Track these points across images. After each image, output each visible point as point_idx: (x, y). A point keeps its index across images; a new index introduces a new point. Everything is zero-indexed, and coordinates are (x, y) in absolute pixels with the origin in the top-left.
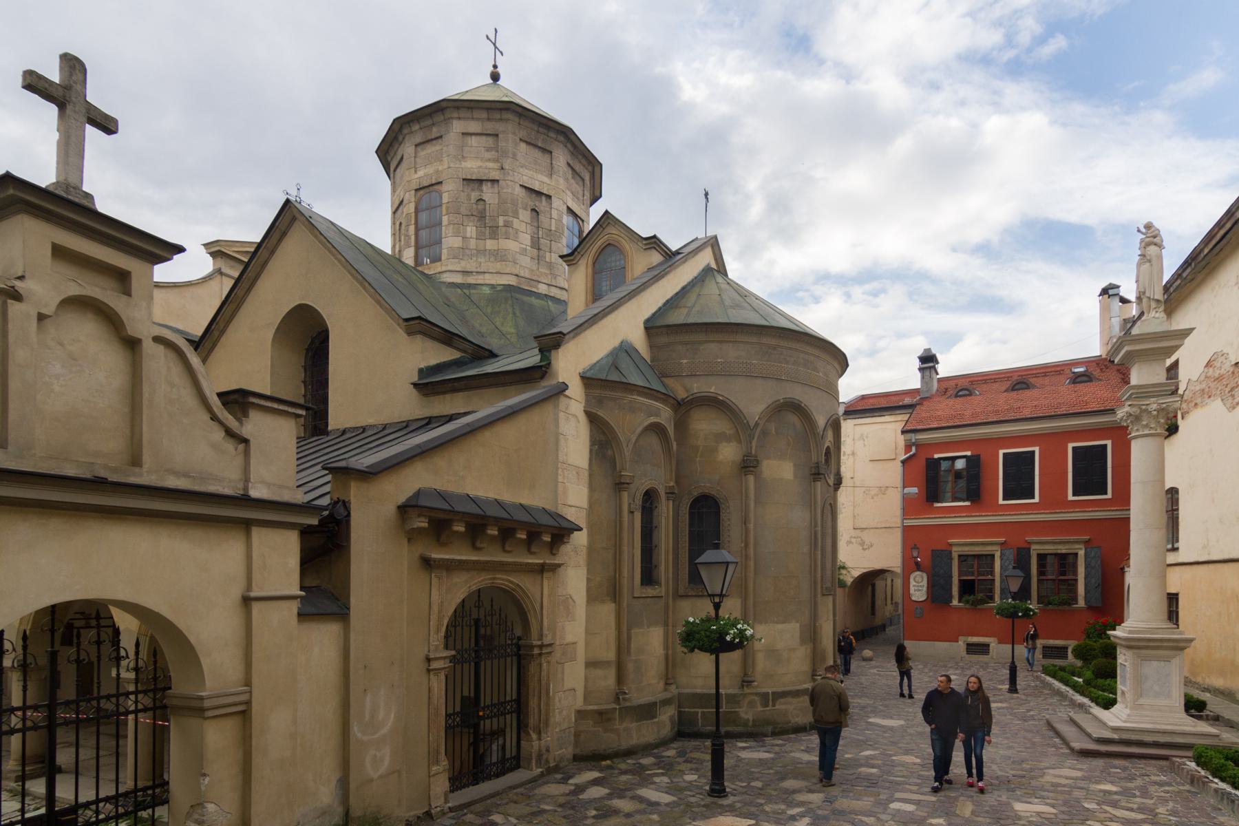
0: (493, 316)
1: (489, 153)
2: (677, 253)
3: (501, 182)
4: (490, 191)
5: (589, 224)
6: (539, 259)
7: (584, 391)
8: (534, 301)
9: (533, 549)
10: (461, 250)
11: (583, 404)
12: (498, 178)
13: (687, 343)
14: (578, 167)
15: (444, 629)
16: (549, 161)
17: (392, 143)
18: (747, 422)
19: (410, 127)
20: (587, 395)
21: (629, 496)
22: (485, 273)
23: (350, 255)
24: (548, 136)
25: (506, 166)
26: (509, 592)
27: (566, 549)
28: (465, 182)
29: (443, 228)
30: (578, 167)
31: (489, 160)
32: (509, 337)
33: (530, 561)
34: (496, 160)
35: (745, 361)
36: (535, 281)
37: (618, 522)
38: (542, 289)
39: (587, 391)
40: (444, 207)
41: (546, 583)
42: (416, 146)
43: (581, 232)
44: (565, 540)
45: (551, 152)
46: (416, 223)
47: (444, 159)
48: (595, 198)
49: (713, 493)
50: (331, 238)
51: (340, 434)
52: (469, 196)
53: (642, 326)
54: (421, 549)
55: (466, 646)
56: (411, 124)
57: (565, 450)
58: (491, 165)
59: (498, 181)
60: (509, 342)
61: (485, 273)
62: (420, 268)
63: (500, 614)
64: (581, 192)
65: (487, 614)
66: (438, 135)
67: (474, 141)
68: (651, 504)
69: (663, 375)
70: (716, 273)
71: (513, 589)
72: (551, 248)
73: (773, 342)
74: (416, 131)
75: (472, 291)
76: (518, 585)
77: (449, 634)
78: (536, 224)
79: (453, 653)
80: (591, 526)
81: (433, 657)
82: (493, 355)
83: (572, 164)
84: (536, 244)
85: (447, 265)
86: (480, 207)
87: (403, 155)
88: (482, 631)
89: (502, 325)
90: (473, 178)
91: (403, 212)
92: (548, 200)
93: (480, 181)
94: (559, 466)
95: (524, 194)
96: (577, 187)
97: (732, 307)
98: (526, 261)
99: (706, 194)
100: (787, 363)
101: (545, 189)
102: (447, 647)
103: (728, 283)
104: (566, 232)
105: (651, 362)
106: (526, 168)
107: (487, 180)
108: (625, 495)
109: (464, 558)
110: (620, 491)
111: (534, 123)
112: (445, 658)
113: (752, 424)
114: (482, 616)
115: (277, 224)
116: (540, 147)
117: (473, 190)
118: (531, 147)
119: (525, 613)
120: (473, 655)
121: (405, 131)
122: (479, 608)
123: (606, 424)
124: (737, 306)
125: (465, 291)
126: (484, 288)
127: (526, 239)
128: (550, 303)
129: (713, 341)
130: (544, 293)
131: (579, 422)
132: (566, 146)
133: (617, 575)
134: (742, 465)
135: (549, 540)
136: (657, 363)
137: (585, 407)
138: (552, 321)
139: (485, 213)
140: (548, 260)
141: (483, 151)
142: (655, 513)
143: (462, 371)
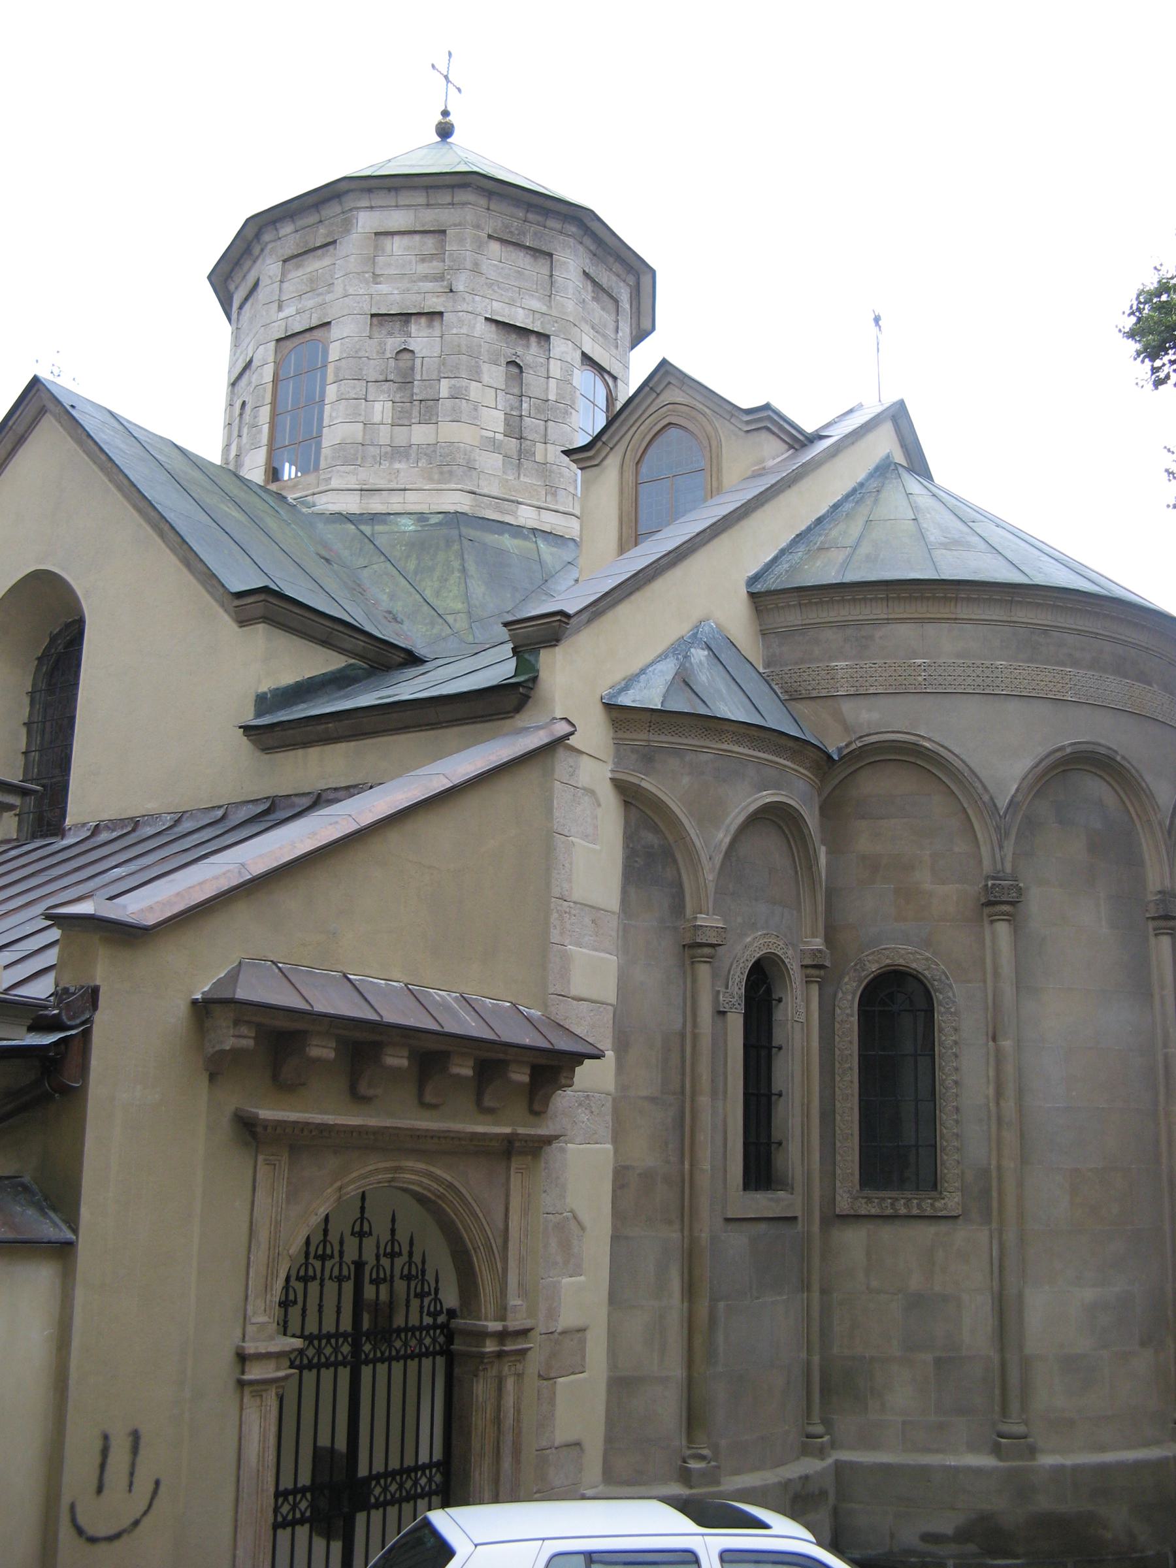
0: (418, 579)
1: (426, 265)
2: (818, 437)
5: (627, 384)
6: (521, 457)
7: (611, 734)
8: (507, 542)
9: (488, 1102)
10: (360, 447)
11: (610, 766)
12: (443, 310)
13: (843, 625)
14: (605, 278)
15: (280, 1283)
16: (545, 271)
17: (239, 260)
18: (992, 798)
19: (276, 230)
20: (618, 744)
21: (715, 976)
22: (405, 490)
23: (138, 473)
24: (545, 227)
25: (460, 286)
26: (434, 1202)
27: (563, 1100)
28: (375, 319)
30: (605, 278)
31: (426, 278)
32: (450, 619)
33: (480, 1129)
35: (978, 662)
36: (512, 501)
37: (689, 1036)
38: (526, 516)
39: (620, 735)
40: (331, 369)
41: (515, 1181)
42: (285, 261)
43: (610, 399)
44: (563, 1081)
45: (551, 255)
46: (274, 403)
47: (336, 282)
48: (640, 335)
49: (914, 965)
50: (107, 443)
51: (89, 834)
52: (382, 344)
53: (743, 592)
54: (233, 1100)
55: (329, 1326)
56: (278, 225)
57: (567, 865)
58: (429, 286)
59: (441, 314)
60: (449, 631)
61: (405, 490)
62: (273, 487)
63: (411, 1254)
64: (612, 325)
65: (382, 1252)
66: (329, 240)
67: (397, 245)
68: (769, 991)
69: (792, 696)
70: (906, 476)
71: (441, 1197)
72: (546, 435)
73: (1043, 618)
74: (286, 236)
75: (379, 528)
76: (450, 1186)
77: (291, 1297)
78: (516, 391)
79: (298, 1343)
80: (622, 1045)
81: (252, 1351)
82: (412, 659)
83: (591, 271)
84: (515, 428)
85: (330, 478)
86: (401, 364)
87: (258, 279)
88: (369, 1292)
89: (437, 594)
91: (250, 383)
92: (543, 343)
93: (406, 317)
94: (552, 906)
95: (494, 336)
96: (600, 314)
97: (945, 546)
98: (491, 462)
99: (877, 320)
100: (1075, 663)
101: (538, 323)
102: (284, 1330)
103: (934, 495)
104: (581, 403)
105: (767, 666)
106: (499, 288)
108: (704, 970)
109: (330, 1119)
110: (693, 963)
111: (518, 207)
112: (278, 1355)
113: (1003, 803)
114: (369, 1256)
115: (10, 423)
116: (528, 248)
117: (390, 334)
118: (511, 248)
119: (466, 1252)
120: (346, 1349)
121: (267, 237)
122: (361, 1235)
123: (658, 806)
124: (952, 544)
125: (363, 528)
126: (404, 520)
127: (494, 421)
128: (542, 545)
129: (902, 620)
130: (532, 524)
131: (599, 805)
132: (581, 243)
133: (687, 1166)
134: (983, 900)
135: (525, 1078)
136: (777, 669)
137: (612, 771)
138: (544, 582)
139: (413, 374)
140: (539, 458)
141: (414, 262)
142: (778, 1015)
143: (347, 697)
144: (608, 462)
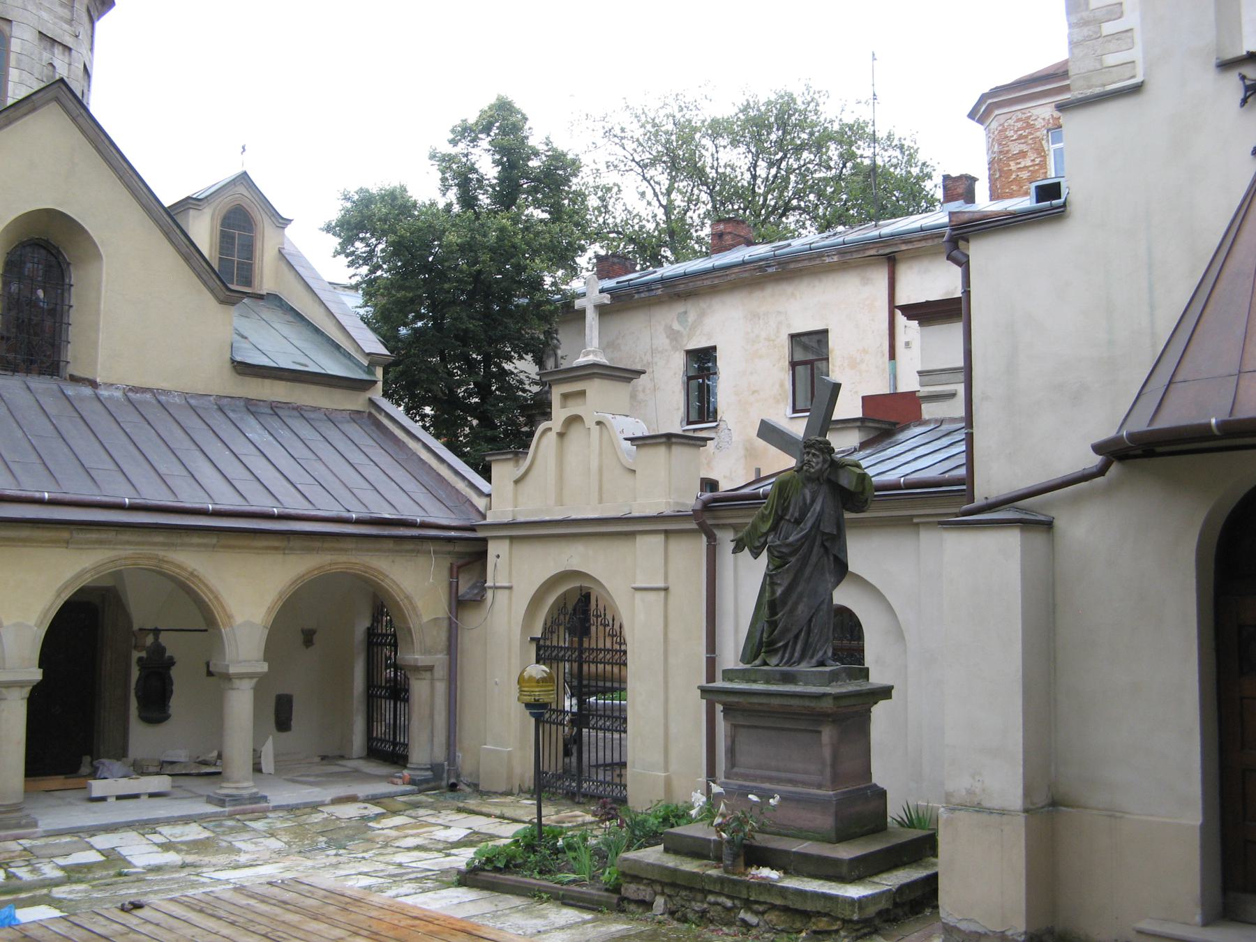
3: (73, 52)
4: (61, 57)
12: (71, 47)
31: (61, 18)
34: (70, 22)
58: (66, 26)
59: (70, 49)
93: (53, 41)
117: (45, 49)
144: (205, 210)
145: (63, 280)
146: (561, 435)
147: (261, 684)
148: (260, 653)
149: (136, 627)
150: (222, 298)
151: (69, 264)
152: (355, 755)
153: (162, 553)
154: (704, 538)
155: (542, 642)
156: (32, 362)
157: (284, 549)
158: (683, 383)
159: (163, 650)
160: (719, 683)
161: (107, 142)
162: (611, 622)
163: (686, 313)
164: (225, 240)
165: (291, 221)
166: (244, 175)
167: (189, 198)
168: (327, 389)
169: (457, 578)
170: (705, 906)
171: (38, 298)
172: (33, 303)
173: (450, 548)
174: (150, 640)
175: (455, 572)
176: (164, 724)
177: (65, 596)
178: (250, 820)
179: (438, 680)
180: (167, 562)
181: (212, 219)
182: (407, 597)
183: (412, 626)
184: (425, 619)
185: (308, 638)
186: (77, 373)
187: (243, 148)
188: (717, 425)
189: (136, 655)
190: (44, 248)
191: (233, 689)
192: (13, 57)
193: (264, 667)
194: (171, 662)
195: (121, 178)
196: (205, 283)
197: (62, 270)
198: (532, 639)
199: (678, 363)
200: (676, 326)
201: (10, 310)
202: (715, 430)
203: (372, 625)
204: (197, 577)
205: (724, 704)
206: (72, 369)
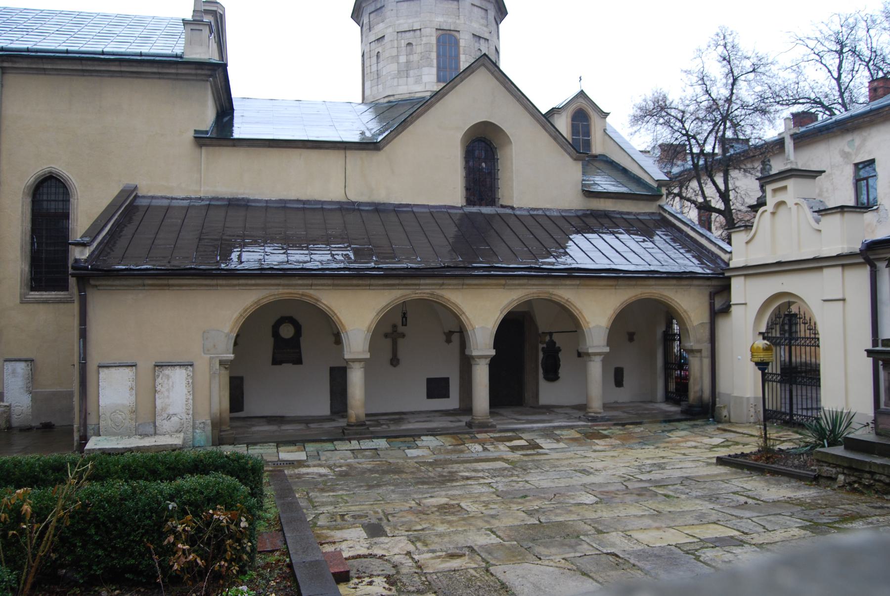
3: (489, 41)
29: (461, 63)
31: (482, 25)
34: (487, 26)
58: (485, 29)
59: (488, 40)
67: (476, 9)
90: (477, 34)
93: (480, 37)
107: (483, 38)
117: (476, 42)
145: (494, 156)
146: (773, 214)
147: (606, 359)
148: (605, 343)
149: (540, 331)
150: (575, 157)
151: (496, 148)
152: (659, 401)
153: (551, 291)
154: (868, 267)
155: (766, 335)
156: (482, 200)
157: (616, 286)
158: (854, 183)
159: (555, 343)
160: (880, 348)
161: (510, 83)
162: (809, 322)
163: (853, 140)
164: (575, 130)
165: (608, 114)
166: (582, 94)
167: (553, 108)
168: (635, 201)
169: (714, 300)
170: (872, 482)
171: (483, 168)
172: (480, 170)
173: (708, 283)
174: (547, 338)
175: (712, 296)
176: (557, 381)
177: (505, 313)
178: (602, 430)
179: (705, 357)
180: (554, 295)
181: (567, 118)
182: (685, 311)
183: (688, 327)
184: (695, 323)
185: (631, 337)
186: (504, 204)
187: (580, 78)
188: (878, 208)
189: (541, 346)
190: (484, 142)
191: (591, 361)
192: (461, 49)
193: (607, 350)
194: (559, 350)
195: (518, 100)
196: (565, 150)
197: (493, 153)
198: (760, 333)
199: (849, 172)
200: (847, 149)
201: (469, 174)
202: (876, 211)
203: (666, 329)
204: (570, 302)
205: (883, 360)
206: (503, 202)
